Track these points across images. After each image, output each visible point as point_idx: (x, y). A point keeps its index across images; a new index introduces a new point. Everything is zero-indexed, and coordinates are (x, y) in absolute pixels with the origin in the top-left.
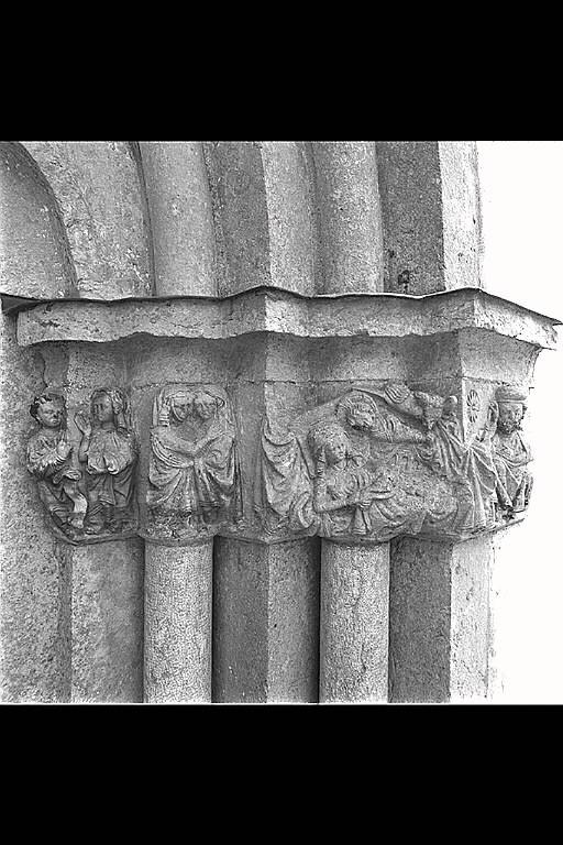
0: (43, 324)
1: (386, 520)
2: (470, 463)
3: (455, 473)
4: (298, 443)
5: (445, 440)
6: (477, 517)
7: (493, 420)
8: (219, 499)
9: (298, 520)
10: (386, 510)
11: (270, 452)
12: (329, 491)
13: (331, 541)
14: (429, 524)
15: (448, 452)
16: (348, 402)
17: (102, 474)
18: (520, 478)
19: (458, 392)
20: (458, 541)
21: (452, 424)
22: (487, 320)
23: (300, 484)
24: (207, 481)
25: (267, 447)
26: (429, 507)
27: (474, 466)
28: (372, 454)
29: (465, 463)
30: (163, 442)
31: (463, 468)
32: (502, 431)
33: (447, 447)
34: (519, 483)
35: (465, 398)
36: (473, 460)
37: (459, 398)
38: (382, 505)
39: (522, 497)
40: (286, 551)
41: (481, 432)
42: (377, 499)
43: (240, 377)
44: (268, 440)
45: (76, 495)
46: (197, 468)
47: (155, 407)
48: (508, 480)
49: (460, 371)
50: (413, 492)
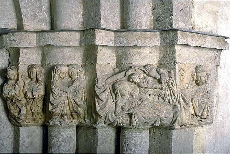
0: (11, 41)
1: (144, 119)
2: (179, 98)
3: (172, 100)
4: (109, 88)
5: (169, 89)
6: (182, 119)
7: (193, 80)
8: (78, 110)
9: (108, 119)
10: (144, 116)
11: (98, 92)
12: (122, 108)
13: (126, 128)
14: (162, 121)
15: (171, 93)
16: (130, 72)
17: (32, 99)
18: (205, 104)
19: (174, 69)
20: (173, 129)
21: (172, 82)
22: (184, 41)
23: (111, 104)
24: (73, 102)
25: (96, 89)
26: (162, 116)
27: (181, 99)
28: (140, 93)
29: (177, 97)
30: (55, 86)
31: (177, 100)
32: (198, 84)
33: (170, 91)
34: (204, 106)
35: (177, 71)
36: (181, 97)
37: (175, 71)
38: (142, 113)
39: (205, 113)
40: (105, 132)
41: (187, 85)
42: (140, 111)
43: (88, 61)
44: (97, 87)
45: (22, 107)
46: (69, 97)
47: (53, 72)
48: (199, 105)
49: (176, 60)
50: (156, 108)
